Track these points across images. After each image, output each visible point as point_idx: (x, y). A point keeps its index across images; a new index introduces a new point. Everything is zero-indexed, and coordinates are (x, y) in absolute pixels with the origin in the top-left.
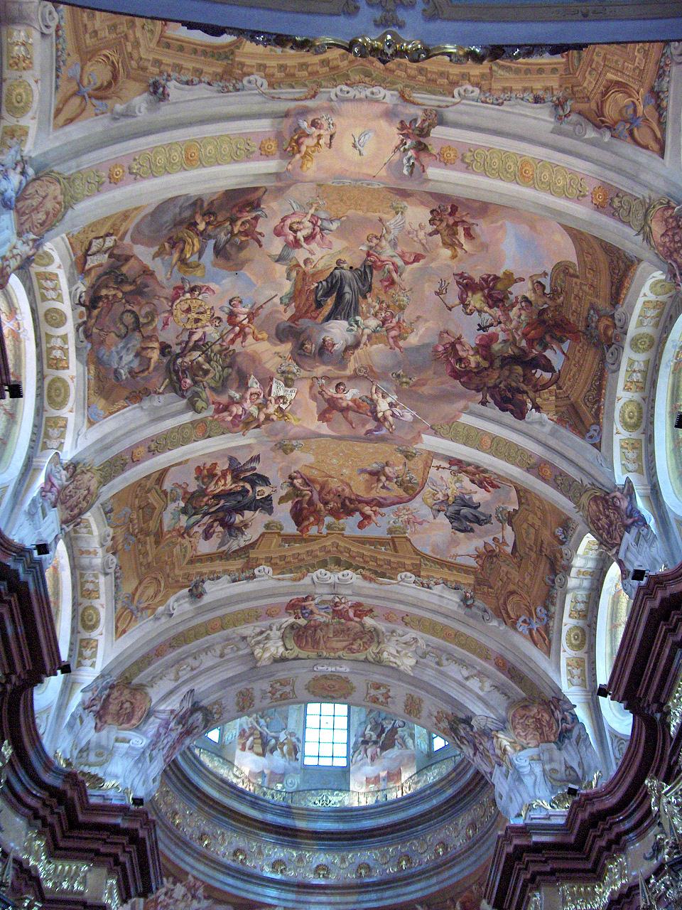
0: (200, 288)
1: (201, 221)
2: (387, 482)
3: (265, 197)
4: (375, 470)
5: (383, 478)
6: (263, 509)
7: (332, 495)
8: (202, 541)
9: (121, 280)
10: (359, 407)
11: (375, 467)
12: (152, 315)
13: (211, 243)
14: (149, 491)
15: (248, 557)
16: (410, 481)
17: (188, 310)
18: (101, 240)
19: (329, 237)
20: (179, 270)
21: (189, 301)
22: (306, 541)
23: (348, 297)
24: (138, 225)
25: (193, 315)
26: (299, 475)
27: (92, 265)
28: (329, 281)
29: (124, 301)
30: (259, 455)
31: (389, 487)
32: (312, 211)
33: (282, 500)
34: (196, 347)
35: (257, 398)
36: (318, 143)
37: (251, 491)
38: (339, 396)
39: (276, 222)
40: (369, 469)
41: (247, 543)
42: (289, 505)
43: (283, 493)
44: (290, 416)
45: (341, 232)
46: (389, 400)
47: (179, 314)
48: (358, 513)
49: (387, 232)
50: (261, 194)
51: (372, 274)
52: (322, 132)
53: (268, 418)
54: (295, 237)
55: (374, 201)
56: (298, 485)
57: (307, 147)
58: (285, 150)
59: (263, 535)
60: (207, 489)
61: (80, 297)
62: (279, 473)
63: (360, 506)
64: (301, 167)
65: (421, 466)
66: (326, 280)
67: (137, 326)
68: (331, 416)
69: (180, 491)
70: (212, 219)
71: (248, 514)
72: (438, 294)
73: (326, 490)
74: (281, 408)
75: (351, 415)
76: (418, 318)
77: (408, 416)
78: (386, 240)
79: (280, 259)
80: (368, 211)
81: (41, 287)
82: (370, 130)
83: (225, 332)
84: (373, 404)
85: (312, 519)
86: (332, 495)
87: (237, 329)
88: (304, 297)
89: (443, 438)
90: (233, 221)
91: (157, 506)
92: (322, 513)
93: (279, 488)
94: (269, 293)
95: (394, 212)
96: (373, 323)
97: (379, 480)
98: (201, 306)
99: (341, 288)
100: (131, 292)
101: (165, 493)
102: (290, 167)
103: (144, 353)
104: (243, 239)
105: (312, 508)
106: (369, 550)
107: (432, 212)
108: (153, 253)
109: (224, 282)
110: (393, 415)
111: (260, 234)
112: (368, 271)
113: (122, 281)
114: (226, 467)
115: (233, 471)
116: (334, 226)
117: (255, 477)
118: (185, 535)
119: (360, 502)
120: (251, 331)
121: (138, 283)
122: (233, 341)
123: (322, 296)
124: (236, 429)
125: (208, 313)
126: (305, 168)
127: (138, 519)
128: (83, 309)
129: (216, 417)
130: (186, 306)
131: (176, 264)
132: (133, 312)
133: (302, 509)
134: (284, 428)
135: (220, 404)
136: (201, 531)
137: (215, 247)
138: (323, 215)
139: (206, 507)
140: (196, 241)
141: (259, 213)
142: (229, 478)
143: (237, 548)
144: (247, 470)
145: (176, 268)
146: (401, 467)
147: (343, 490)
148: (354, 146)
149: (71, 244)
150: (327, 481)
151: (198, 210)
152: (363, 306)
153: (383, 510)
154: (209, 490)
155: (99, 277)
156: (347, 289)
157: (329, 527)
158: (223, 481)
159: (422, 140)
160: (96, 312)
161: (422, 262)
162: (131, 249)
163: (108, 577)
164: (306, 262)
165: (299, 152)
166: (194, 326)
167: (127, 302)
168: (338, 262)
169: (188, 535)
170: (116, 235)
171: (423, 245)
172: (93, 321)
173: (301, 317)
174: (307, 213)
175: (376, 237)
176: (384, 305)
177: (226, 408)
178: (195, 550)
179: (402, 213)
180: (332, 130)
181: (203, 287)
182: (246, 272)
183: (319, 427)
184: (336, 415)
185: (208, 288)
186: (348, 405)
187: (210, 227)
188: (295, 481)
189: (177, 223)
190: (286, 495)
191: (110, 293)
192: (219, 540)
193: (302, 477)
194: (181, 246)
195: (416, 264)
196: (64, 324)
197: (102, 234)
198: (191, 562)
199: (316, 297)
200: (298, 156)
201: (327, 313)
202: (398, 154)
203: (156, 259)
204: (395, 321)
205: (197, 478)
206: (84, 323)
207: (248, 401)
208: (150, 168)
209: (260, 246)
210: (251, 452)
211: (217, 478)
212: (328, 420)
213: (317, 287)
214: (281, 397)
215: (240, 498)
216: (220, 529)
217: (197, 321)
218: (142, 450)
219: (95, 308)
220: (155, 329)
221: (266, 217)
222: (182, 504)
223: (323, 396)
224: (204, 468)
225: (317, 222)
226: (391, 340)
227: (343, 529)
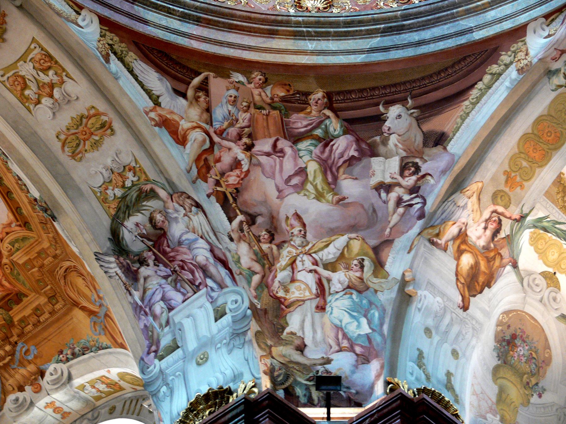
163: (73, 372)
178: (9, 225)
198: (25, 224)
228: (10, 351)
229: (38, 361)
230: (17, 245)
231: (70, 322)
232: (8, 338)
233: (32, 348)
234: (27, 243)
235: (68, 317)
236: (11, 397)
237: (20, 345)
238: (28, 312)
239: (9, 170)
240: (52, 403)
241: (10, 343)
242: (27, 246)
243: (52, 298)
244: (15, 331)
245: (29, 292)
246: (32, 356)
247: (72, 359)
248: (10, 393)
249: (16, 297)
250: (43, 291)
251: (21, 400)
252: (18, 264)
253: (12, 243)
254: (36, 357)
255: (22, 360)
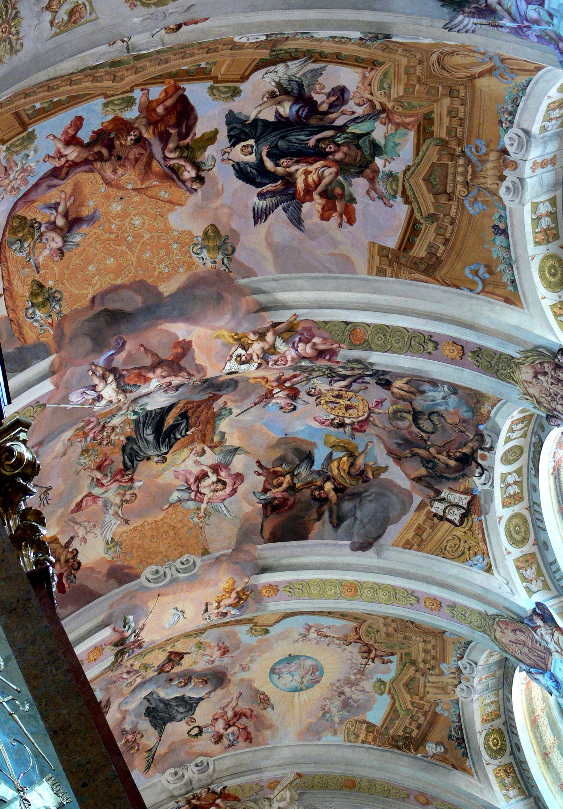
0: (331, 424)
1: (329, 492)
2: (52, 218)
3: (260, 519)
4: (75, 229)
5: (60, 222)
6: (242, 122)
7: (131, 156)
8: (352, 88)
9: (427, 462)
10: (140, 376)
11: (76, 238)
12: (396, 415)
13: (317, 467)
14: (432, 218)
15: (272, 51)
16: (21, 241)
17: (348, 408)
18: (448, 517)
19: (180, 483)
20: (357, 448)
21: (348, 415)
22: (170, 75)
23: (149, 431)
24: (404, 512)
25: (343, 402)
26: (189, 185)
27: (463, 496)
28: (173, 440)
29: (429, 443)
30: (256, 223)
31: (48, 212)
32: (203, 506)
33: (211, 138)
34: (344, 378)
35: (277, 361)
36: (219, 603)
37: (264, 153)
38: (167, 380)
39: (242, 488)
40: (84, 228)
41: (272, 68)
42: (200, 130)
43: (211, 151)
44: (231, 340)
45: (166, 491)
46: (103, 402)
47: (361, 407)
48: (86, 140)
49: (117, 513)
50: (265, 524)
51: (124, 463)
52: (216, 611)
53: (262, 336)
54: (218, 474)
55: (139, 542)
56: (189, 167)
57: (230, 597)
58: (252, 591)
59: (244, 78)
60: (337, 174)
61: (481, 474)
62: (220, 187)
63: (85, 154)
64: (235, 582)
65: (16, 283)
66: (177, 440)
67: (416, 415)
68: (175, 351)
69: (381, 186)
70: (317, 493)
71: (269, 115)
72: (50, 489)
73: (141, 165)
74: (244, 348)
75: (148, 361)
76: (65, 454)
77: (76, 398)
78: (116, 504)
79: (235, 451)
80: (143, 526)
81: (521, 487)
82: (169, 628)
83: (305, 383)
84: (122, 389)
85: (160, 110)
86: (131, 156)
87: (287, 384)
88: (202, 418)
89: (30, 405)
90: (292, 488)
91: (422, 183)
92: (144, 121)
93: (219, 157)
94: (247, 417)
95: (116, 539)
96: (116, 421)
97: (66, 215)
98: (332, 409)
99: (157, 438)
100: (419, 447)
101: (407, 201)
102: (247, 580)
103: (412, 389)
104: (279, 469)
105: (161, 127)
106: (62, 94)
107: (79, 564)
108: (387, 473)
109: (302, 428)
110: (94, 387)
111: (259, 474)
112: (129, 464)
113: (429, 461)
114: (306, 207)
115: (293, 196)
116: (175, 496)
117: (258, 180)
118: (379, 107)
119: (86, 162)
120: (269, 383)
121: (408, 452)
122: (294, 376)
123: (180, 425)
124: (308, 325)
125: (323, 402)
126: (231, 582)
127: (455, 174)
128: (479, 461)
129: (335, 346)
130: (351, 411)
131: (360, 455)
132: (419, 428)
133: (178, 125)
134: (239, 323)
135: (329, 360)
136: (351, 103)
137: (312, 462)
138: (191, 505)
139: (340, 141)
140: (336, 472)
141: (263, 497)
142: (300, 185)
143: (289, 63)
144: (273, 193)
145: (361, 450)
146: (41, 259)
147: (115, 171)
148: (183, 612)
149: (485, 542)
150: (143, 182)
151: (334, 507)
152: (129, 430)
153: (48, 166)
154: (333, 170)
155: (455, 479)
156: (151, 438)
157: (130, 102)
158: (310, 180)
159: (121, 648)
160: (466, 450)
161: (73, 506)
162: (412, 486)
163: (525, 126)
164: (203, 452)
165: (237, 592)
166: (343, 393)
167: (426, 441)
168: (164, 460)
169: (373, 105)
170: (429, 512)
171: (76, 523)
172: (470, 444)
173: (206, 400)
174: (208, 503)
175: (127, 501)
176: (105, 442)
177: (321, 354)
178: (364, 77)
179: (107, 543)
180: (206, 616)
181: (328, 426)
182: (276, 436)
183: (189, 333)
184: (166, 354)
185: (322, 423)
186: (154, 372)
187: (319, 483)
188: (193, 174)
189: (356, 496)
190: (204, 148)
191: (445, 458)
192: (320, 79)
193: (184, 182)
194: (353, 471)
195: (78, 499)
196: (505, 453)
197: (447, 525)
198: (374, 64)
199: (187, 422)
200: (239, 589)
201: (174, 410)
202: (140, 625)
203: (384, 466)
204: (91, 435)
205: (352, 200)
206: (482, 449)
207: (289, 358)
208: (396, 594)
209: (258, 462)
210: (269, 233)
211: (320, 188)
212: (178, 344)
213: (187, 430)
214: (243, 363)
215: (282, 144)
216: (319, 98)
217: (339, 397)
218: (447, 350)
219: (465, 454)
220: (394, 403)
221: (254, 493)
222: (379, 162)
223: (189, 374)
224: (341, 216)
225: (196, 495)
226: (93, 419)
227: (106, 105)
228: (465, 162)
229: (492, 146)
230: (385, 86)
231: (483, 94)
232: (453, 155)
233: (478, 142)
234: (391, 75)
235: (478, 93)
236: (502, 192)
237: (467, 150)
238: (446, 121)
239: (319, 40)
240: (535, 163)
241: (459, 157)
242: (393, 77)
243: (451, 93)
244: (453, 144)
245: (431, 107)
246: (484, 148)
247: (514, 118)
248: (498, 189)
249: (426, 121)
250: (439, 95)
251: (511, 186)
252: (401, 97)
253: (381, 88)
254: (487, 146)
255: (480, 158)
